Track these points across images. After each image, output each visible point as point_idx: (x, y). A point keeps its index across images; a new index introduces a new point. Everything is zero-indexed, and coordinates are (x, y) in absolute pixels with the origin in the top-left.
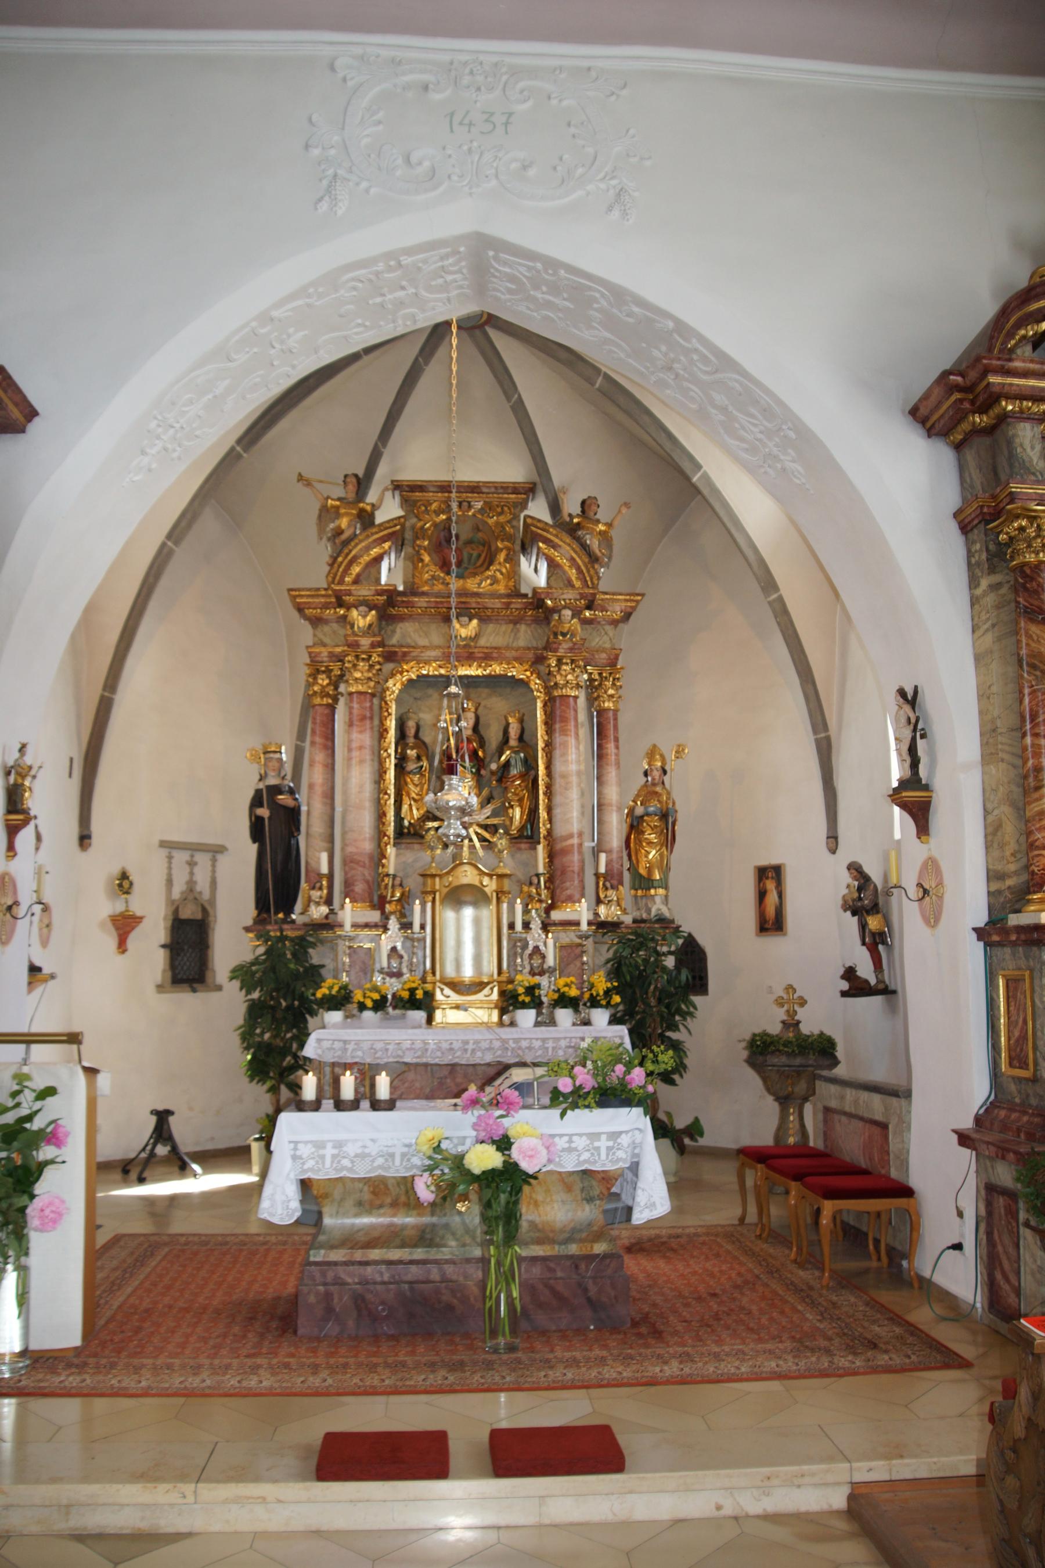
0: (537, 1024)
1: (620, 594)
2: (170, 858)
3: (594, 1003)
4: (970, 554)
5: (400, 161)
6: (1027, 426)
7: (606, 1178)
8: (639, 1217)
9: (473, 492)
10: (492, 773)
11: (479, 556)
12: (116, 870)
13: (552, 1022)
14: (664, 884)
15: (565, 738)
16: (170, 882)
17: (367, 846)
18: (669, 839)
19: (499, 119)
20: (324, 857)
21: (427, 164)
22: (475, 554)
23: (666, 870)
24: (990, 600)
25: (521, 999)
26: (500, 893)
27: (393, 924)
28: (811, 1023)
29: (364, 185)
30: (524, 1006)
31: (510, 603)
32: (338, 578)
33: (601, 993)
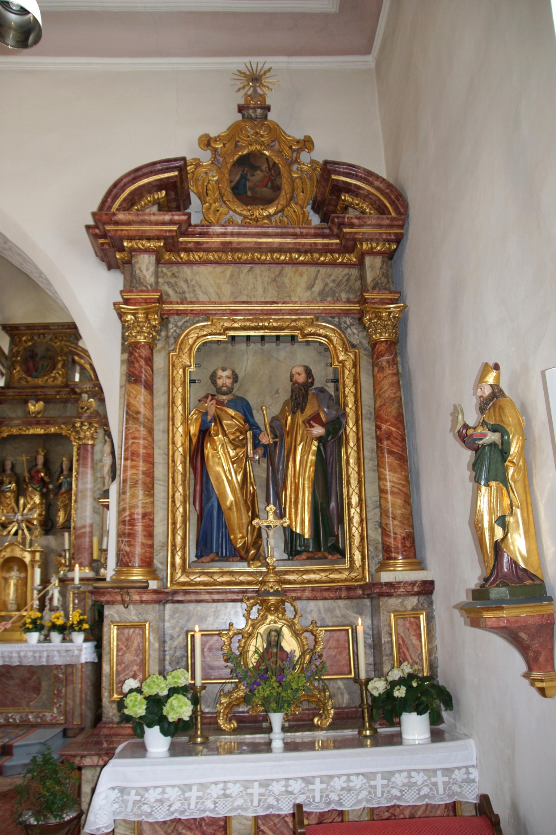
0: (39, 641)
3: (72, 628)
6: (146, 256)
9: (45, 329)
11: (48, 365)
15: (84, 469)
22: (46, 364)
25: (27, 626)
26: (33, 561)
31: (60, 391)
33: (75, 622)
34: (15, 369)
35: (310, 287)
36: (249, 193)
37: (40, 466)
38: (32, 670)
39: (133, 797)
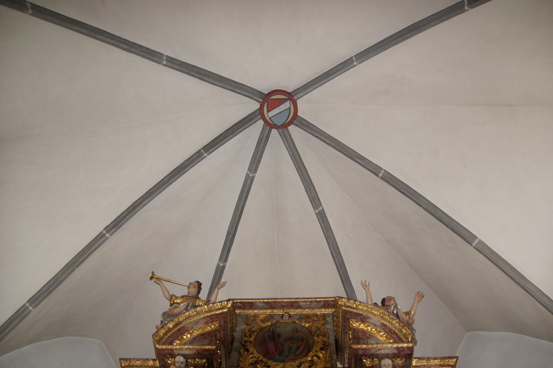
1: (435, 359)
11: (298, 347)
22: (295, 346)
32: (164, 340)
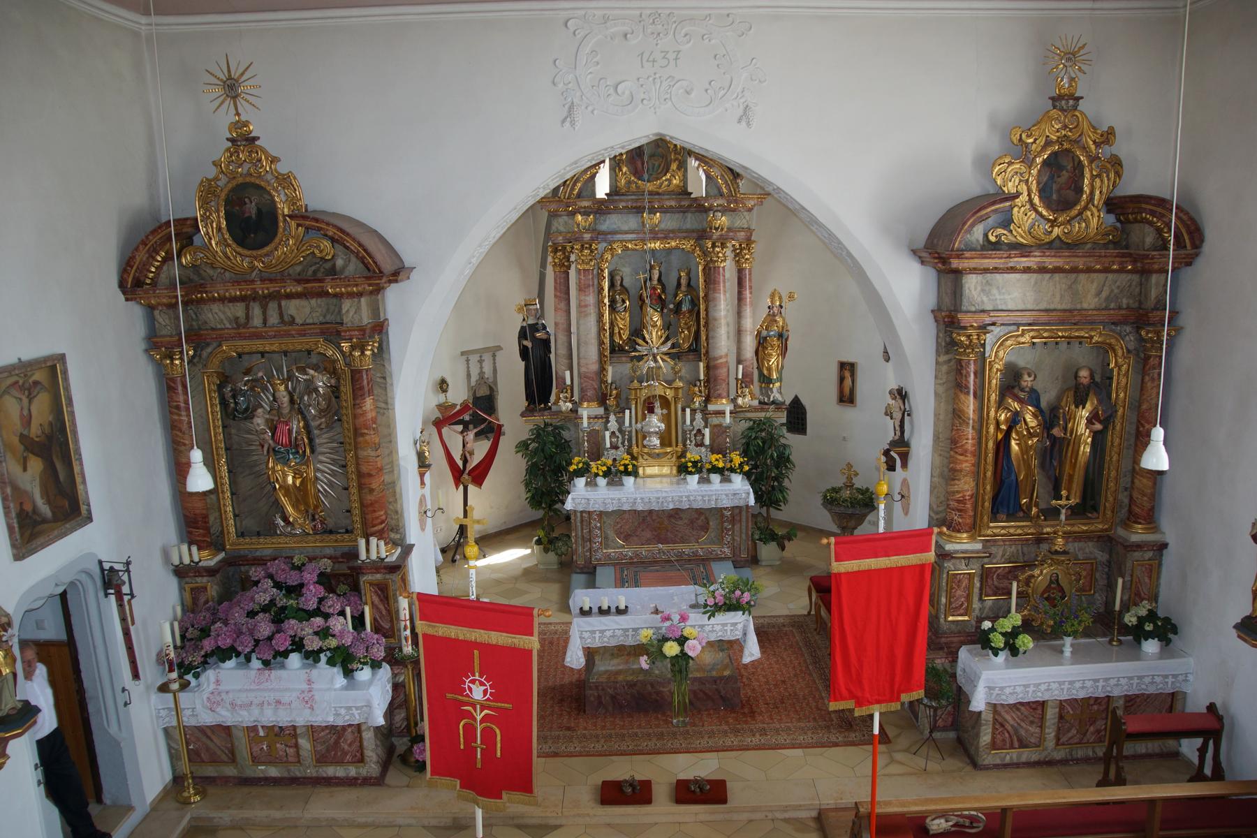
2: (468, 361)
3: (732, 470)
4: (938, 337)
5: (612, 91)
7: (731, 643)
8: (747, 659)
10: (671, 310)
12: (438, 377)
13: (708, 481)
14: (780, 379)
16: (469, 376)
17: (594, 367)
18: (784, 351)
19: (671, 56)
20: (568, 373)
21: (627, 92)
23: (780, 372)
24: (944, 368)
26: (676, 398)
27: (612, 418)
28: (859, 483)
29: (590, 108)
30: (691, 473)
34: (621, 170)
35: (1098, 294)
36: (1054, 197)
37: (655, 282)
38: (700, 512)
39: (997, 691)
